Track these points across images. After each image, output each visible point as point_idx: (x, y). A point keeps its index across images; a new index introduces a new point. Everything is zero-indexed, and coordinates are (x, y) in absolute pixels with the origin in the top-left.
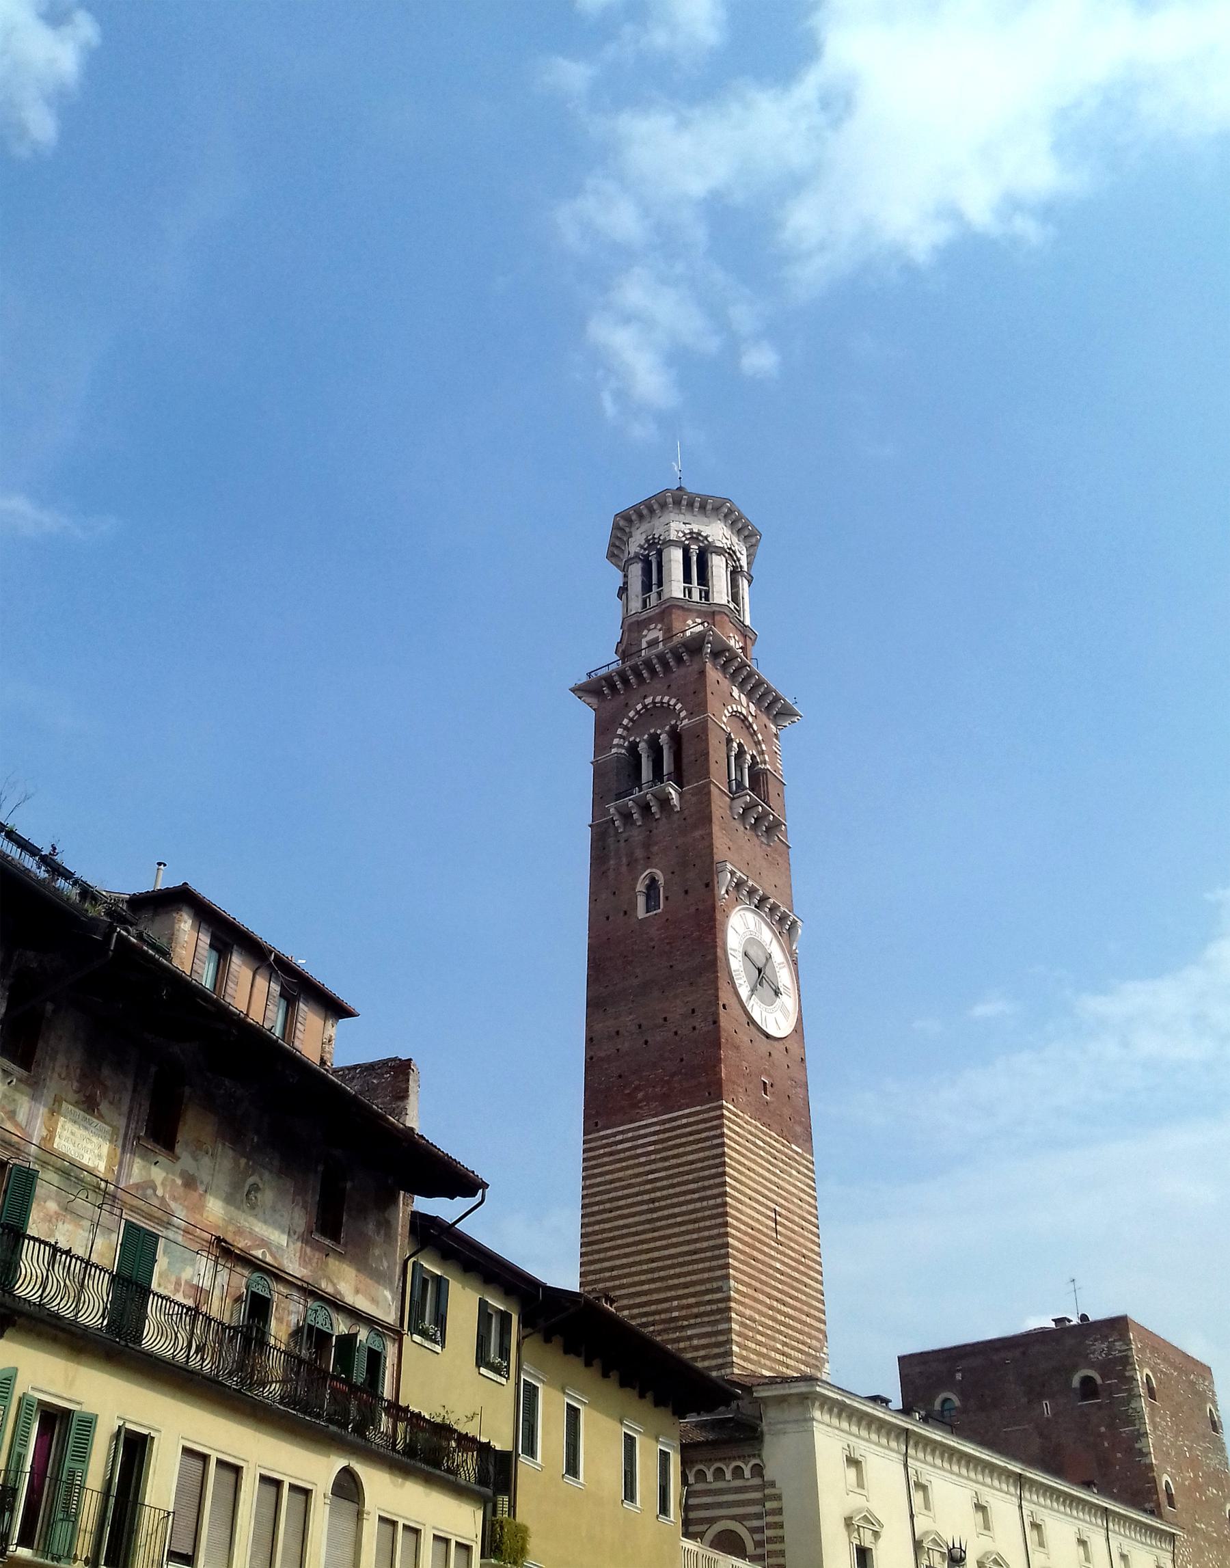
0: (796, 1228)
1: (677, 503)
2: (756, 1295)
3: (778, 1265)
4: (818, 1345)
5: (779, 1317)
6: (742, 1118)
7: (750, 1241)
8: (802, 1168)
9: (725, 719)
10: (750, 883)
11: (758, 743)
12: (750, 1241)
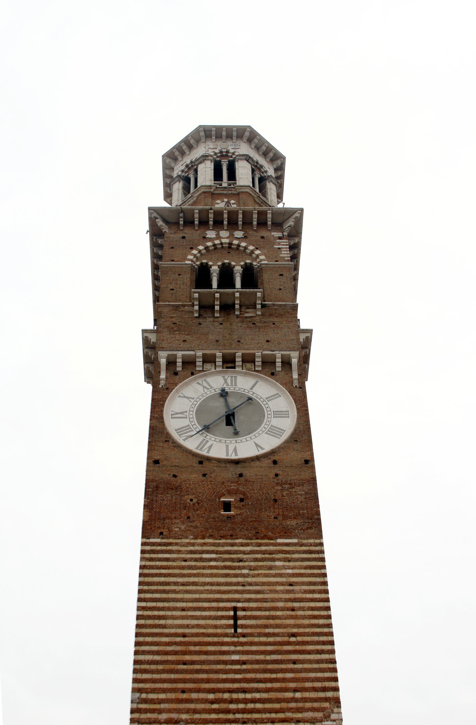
0: (279, 613)
1: (176, 159)
2: (185, 696)
3: (235, 657)
4: (319, 715)
5: (233, 706)
6: (177, 544)
7: (179, 648)
8: (296, 556)
9: (190, 257)
10: (199, 353)
11: (252, 252)
12: (179, 648)
